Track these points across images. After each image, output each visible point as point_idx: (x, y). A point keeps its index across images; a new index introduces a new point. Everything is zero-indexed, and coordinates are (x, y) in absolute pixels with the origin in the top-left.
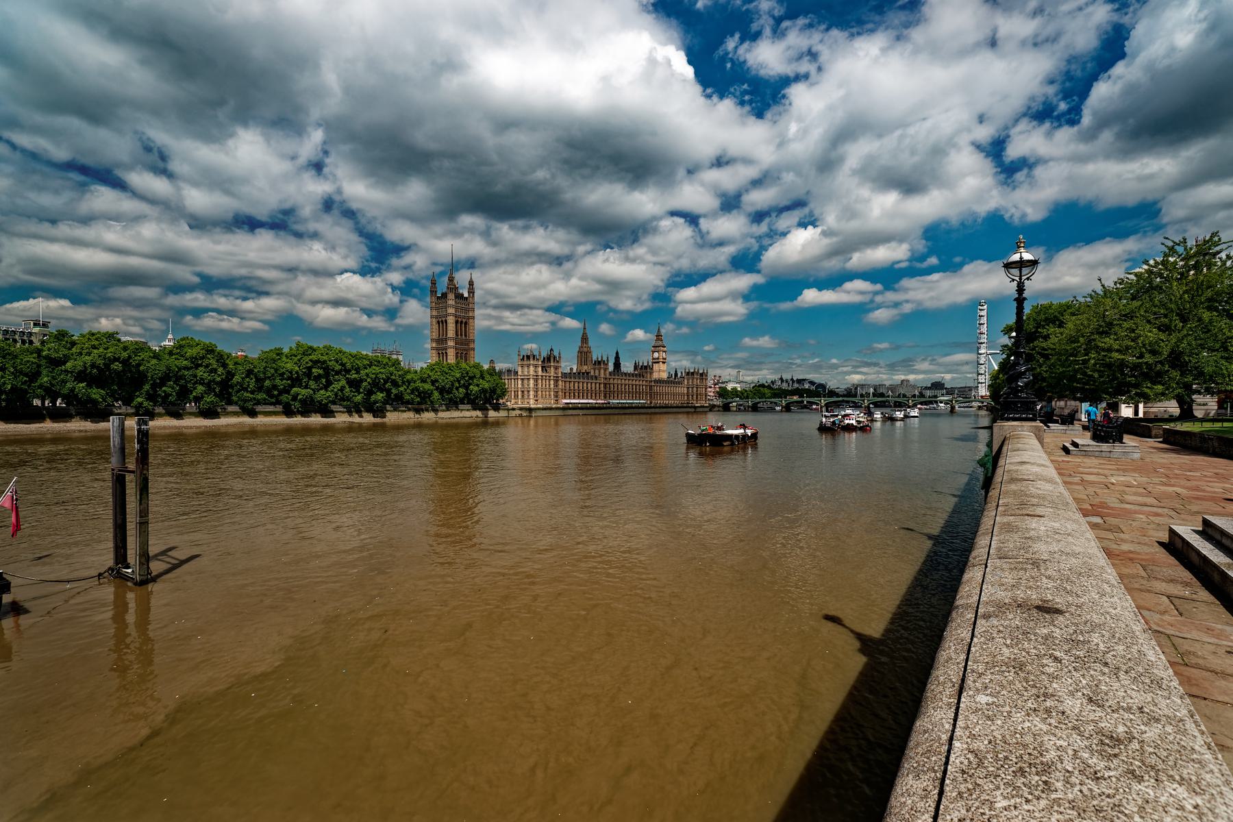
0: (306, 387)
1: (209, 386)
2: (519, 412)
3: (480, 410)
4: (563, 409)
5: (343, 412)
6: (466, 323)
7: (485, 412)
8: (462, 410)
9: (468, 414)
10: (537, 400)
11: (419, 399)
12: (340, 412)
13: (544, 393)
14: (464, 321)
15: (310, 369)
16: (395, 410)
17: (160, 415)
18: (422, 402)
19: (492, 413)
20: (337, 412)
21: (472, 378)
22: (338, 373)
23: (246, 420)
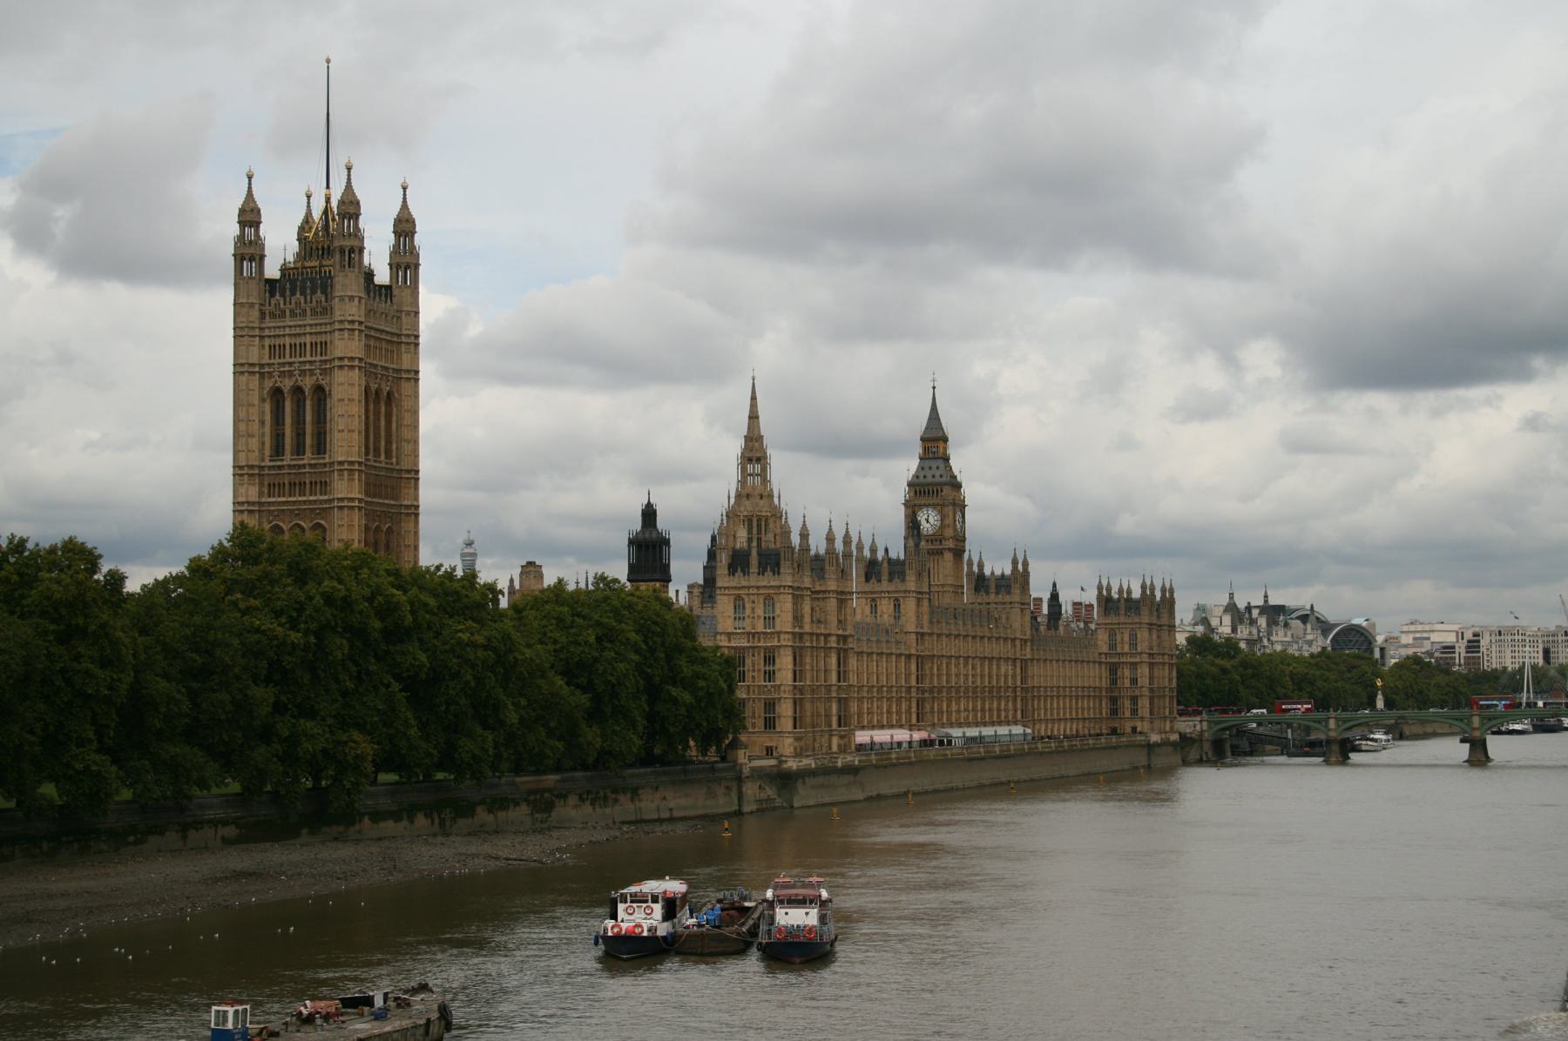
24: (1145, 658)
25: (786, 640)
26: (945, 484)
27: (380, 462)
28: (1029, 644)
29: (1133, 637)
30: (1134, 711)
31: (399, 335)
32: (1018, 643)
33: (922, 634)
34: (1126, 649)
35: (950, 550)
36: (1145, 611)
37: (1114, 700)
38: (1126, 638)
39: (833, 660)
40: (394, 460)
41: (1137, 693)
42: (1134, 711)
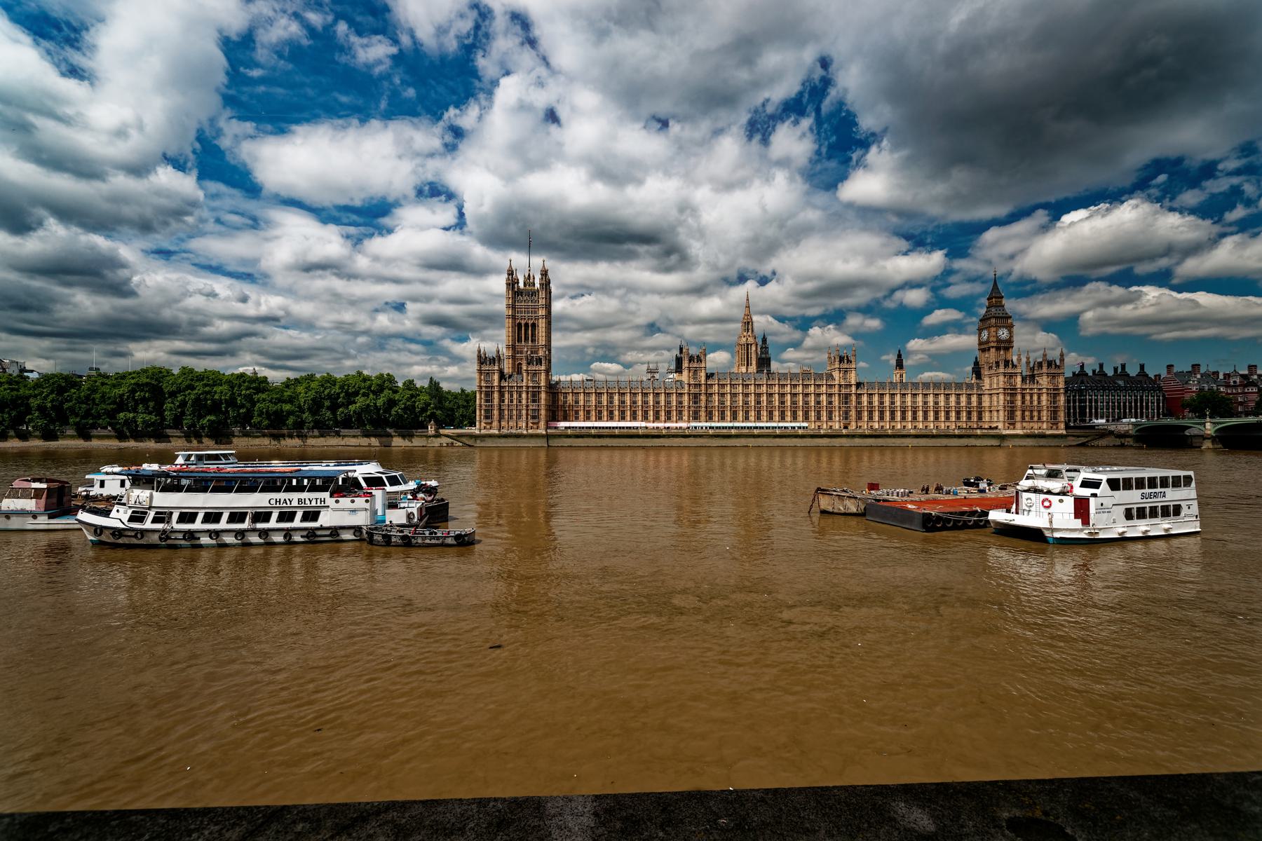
0: (135, 410)
1: (41, 409)
2: (450, 440)
3: (375, 436)
4: (548, 437)
5: (179, 437)
7: (384, 439)
8: (344, 436)
9: (353, 441)
10: (491, 423)
11: (266, 422)
12: (176, 436)
13: (506, 412)
15: (133, 391)
16: (246, 435)
17: (12, 437)
18: (276, 424)
19: (398, 442)
20: (172, 436)
21: (356, 394)
22: (173, 394)
23: (80, 443)
30: (998, 417)
39: (524, 395)
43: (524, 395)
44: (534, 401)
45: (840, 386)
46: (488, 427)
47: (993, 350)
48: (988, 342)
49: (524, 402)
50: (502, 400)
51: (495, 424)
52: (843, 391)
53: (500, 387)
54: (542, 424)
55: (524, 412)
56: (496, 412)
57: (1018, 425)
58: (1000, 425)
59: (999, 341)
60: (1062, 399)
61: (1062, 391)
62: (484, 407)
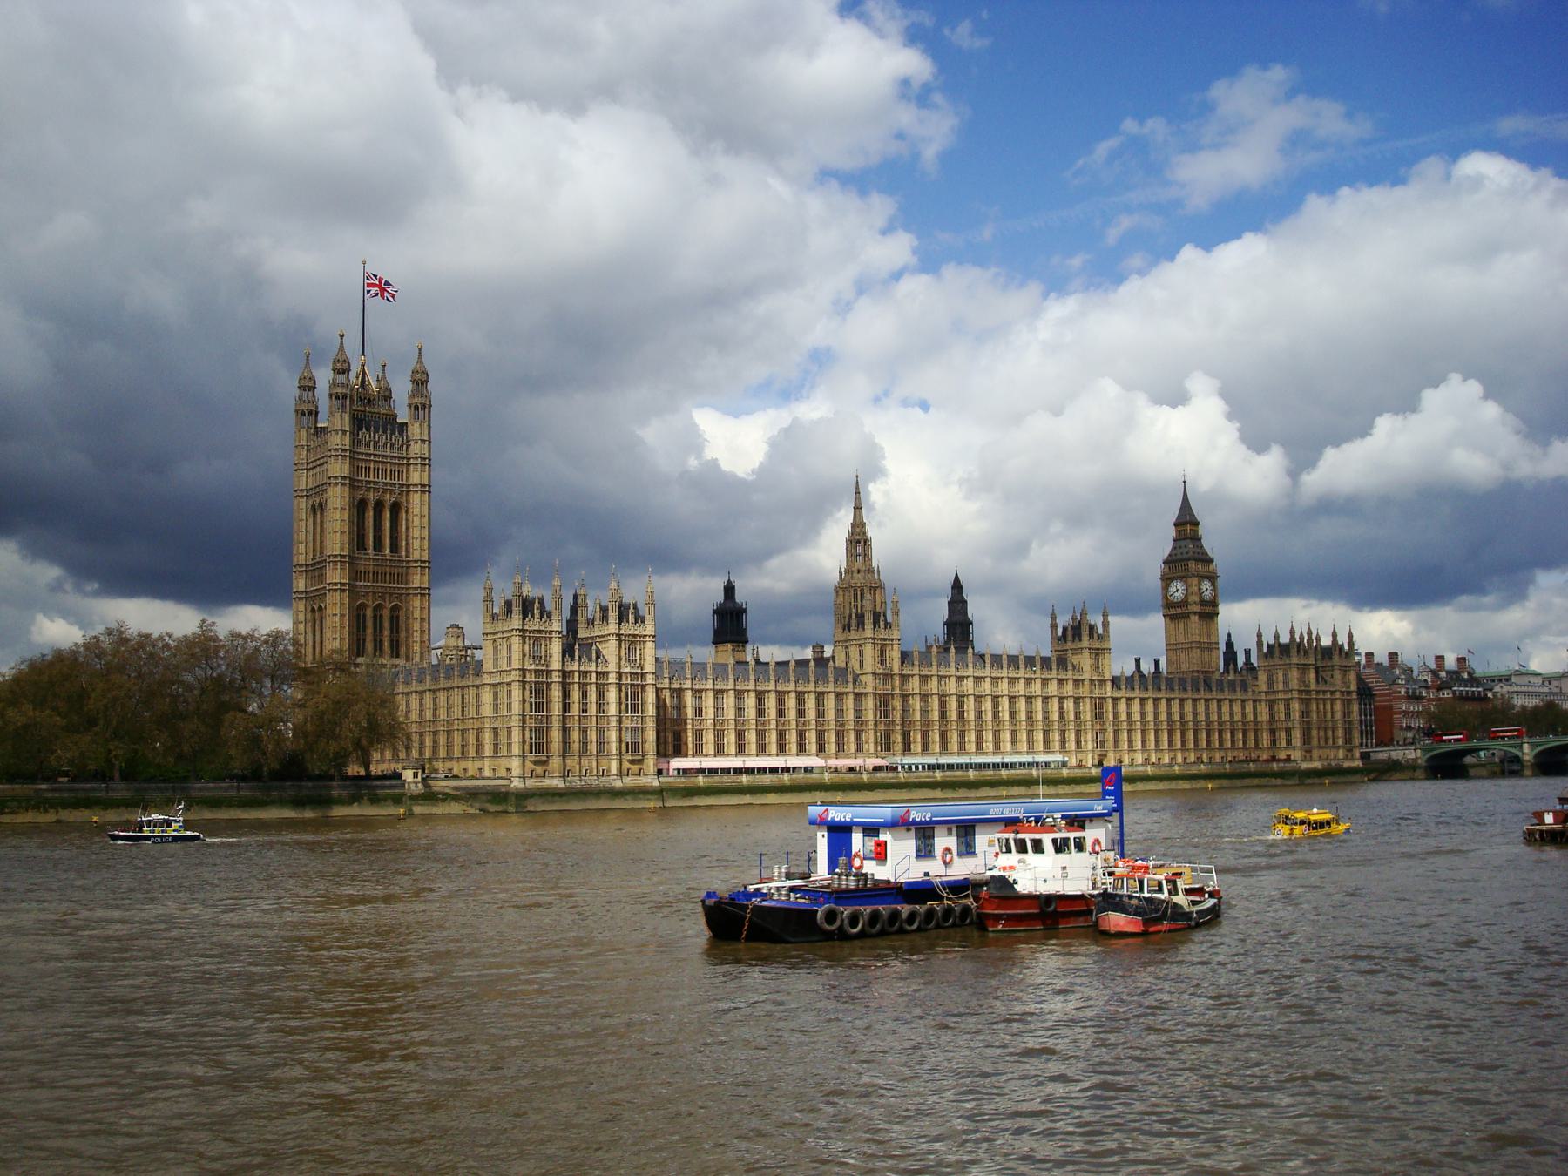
6: (396, 508)
14: (389, 499)
24: (1295, 694)
25: (515, 676)
26: (1189, 559)
27: (385, 555)
28: (1109, 684)
29: (1286, 675)
30: (1289, 742)
31: (409, 459)
32: (1087, 682)
33: (885, 675)
34: (1281, 687)
35: (1195, 613)
36: (1294, 651)
37: (1273, 732)
38: (1281, 678)
39: (612, 695)
40: (404, 553)
41: (1290, 725)
42: (1289, 742)
43: (612, 695)
44: (634, 709)
45: (1092, 681)
46: (539, 770)
47: (1195, 618)
48: (1184, 603)
49: (612, 709)
50: (566, 708)
51: (555, 763)
52: (1097, 693)
53: (565, 674)
54: (651, 764)
55: (613, 735)
56: (556, 735)
57: (1316, 753)
58: (1296, 755)
59: (1203, 603)
60: (1355, 707)
61: (1354, 695)
62: (531, 723)
